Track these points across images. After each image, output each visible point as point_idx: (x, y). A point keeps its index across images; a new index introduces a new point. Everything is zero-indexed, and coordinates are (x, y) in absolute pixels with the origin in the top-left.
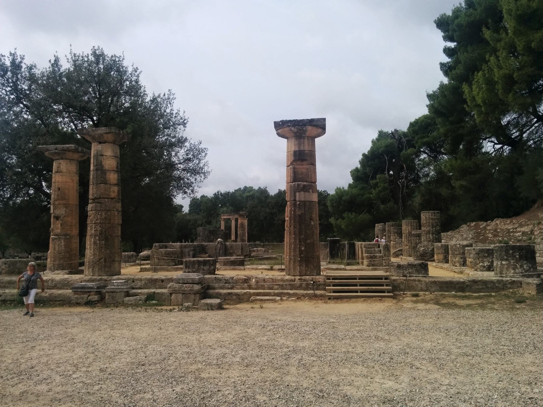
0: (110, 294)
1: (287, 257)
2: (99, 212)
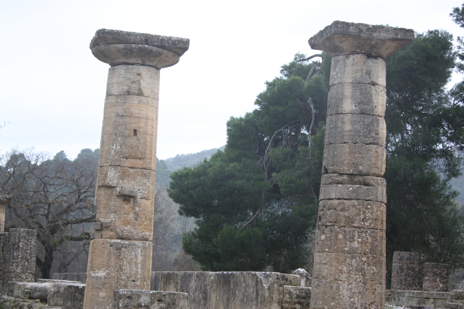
2: (369, 204)
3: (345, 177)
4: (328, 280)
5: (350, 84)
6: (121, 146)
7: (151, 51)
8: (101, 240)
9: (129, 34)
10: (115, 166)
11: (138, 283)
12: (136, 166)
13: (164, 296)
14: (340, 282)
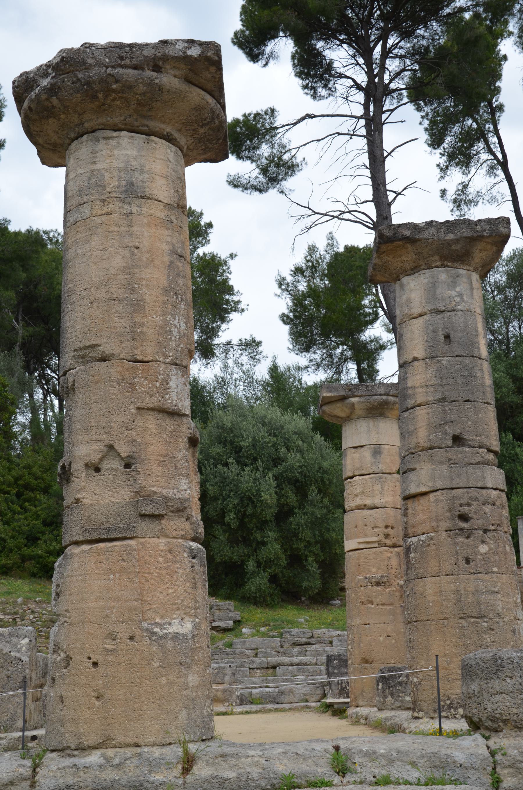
4: (506, 620)
6: (186, 324)
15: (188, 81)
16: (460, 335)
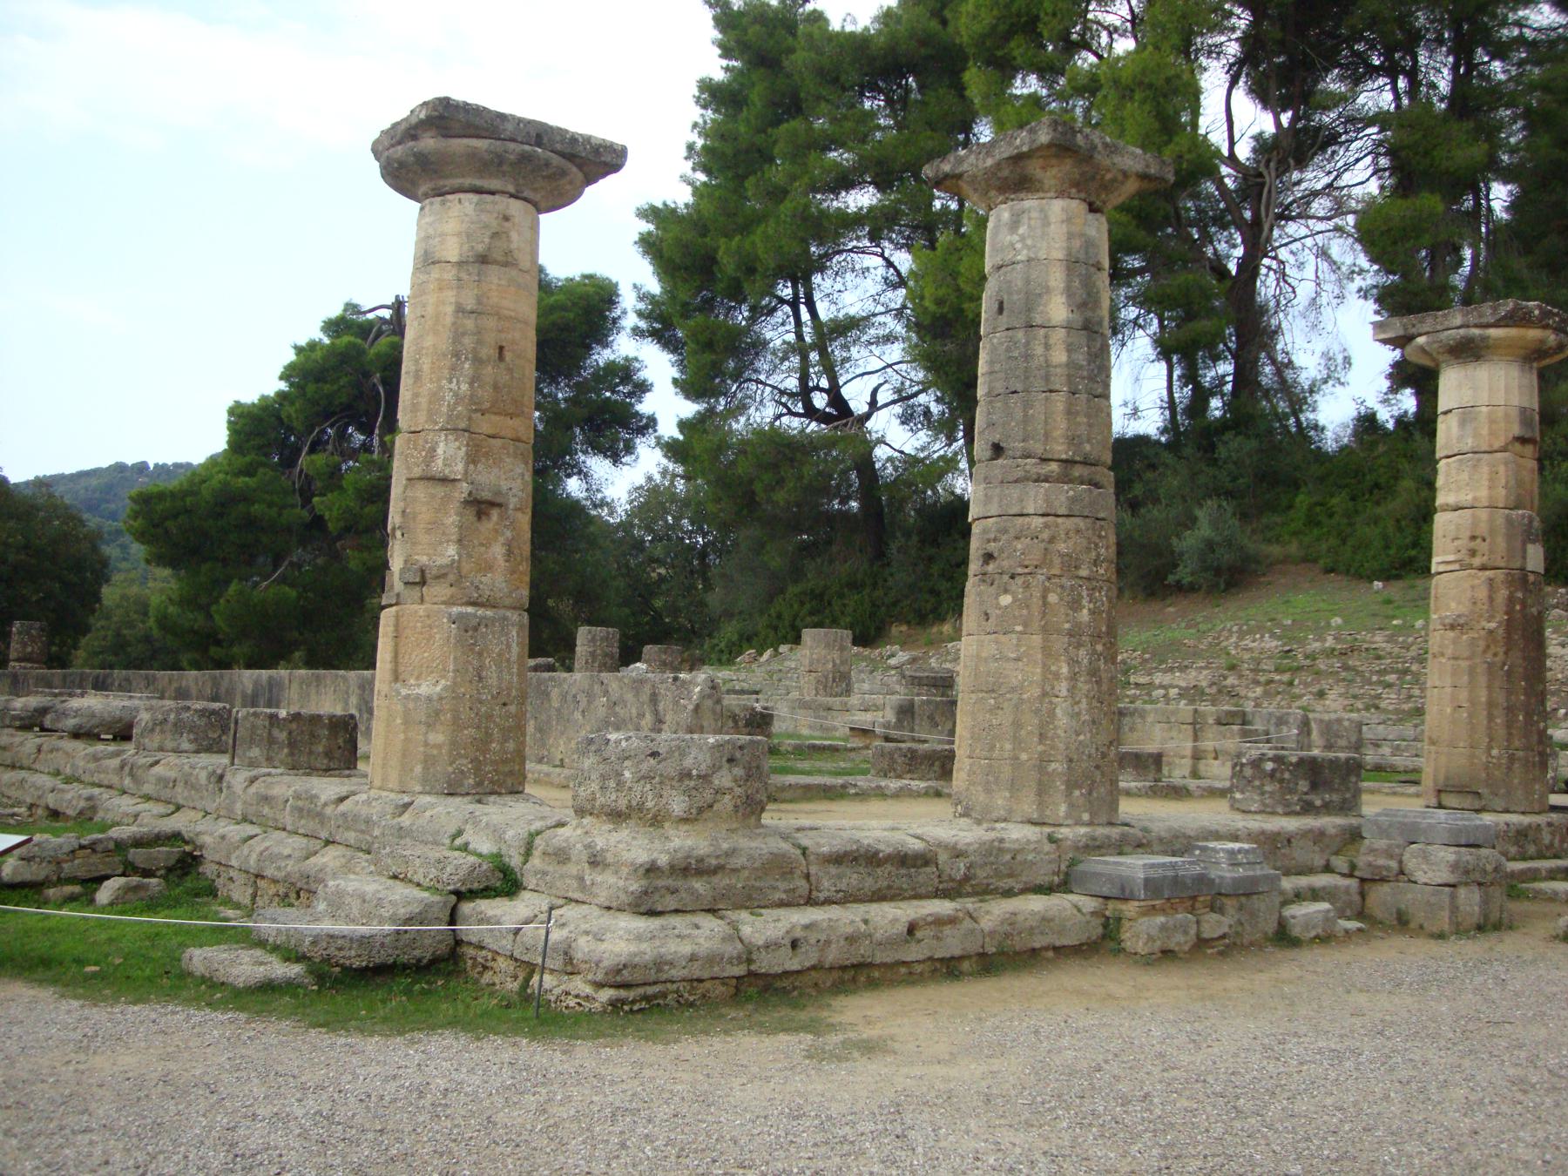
0: (1243, 899)
1: (1495, 752)
3: (1054, 466)
4: (1025, 696)
5: (1059, 263)
6: (471, 384)
7: (547, 164)
8: (421, 610)
9: (502, 117)
10: (455, 430)
11: (513, 708)
12: (502, 434)
13: (741, 748)
14: (1055, 700)
15: (446, 136)
16: (1015, 297)
